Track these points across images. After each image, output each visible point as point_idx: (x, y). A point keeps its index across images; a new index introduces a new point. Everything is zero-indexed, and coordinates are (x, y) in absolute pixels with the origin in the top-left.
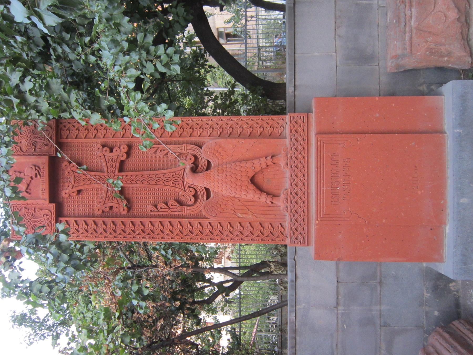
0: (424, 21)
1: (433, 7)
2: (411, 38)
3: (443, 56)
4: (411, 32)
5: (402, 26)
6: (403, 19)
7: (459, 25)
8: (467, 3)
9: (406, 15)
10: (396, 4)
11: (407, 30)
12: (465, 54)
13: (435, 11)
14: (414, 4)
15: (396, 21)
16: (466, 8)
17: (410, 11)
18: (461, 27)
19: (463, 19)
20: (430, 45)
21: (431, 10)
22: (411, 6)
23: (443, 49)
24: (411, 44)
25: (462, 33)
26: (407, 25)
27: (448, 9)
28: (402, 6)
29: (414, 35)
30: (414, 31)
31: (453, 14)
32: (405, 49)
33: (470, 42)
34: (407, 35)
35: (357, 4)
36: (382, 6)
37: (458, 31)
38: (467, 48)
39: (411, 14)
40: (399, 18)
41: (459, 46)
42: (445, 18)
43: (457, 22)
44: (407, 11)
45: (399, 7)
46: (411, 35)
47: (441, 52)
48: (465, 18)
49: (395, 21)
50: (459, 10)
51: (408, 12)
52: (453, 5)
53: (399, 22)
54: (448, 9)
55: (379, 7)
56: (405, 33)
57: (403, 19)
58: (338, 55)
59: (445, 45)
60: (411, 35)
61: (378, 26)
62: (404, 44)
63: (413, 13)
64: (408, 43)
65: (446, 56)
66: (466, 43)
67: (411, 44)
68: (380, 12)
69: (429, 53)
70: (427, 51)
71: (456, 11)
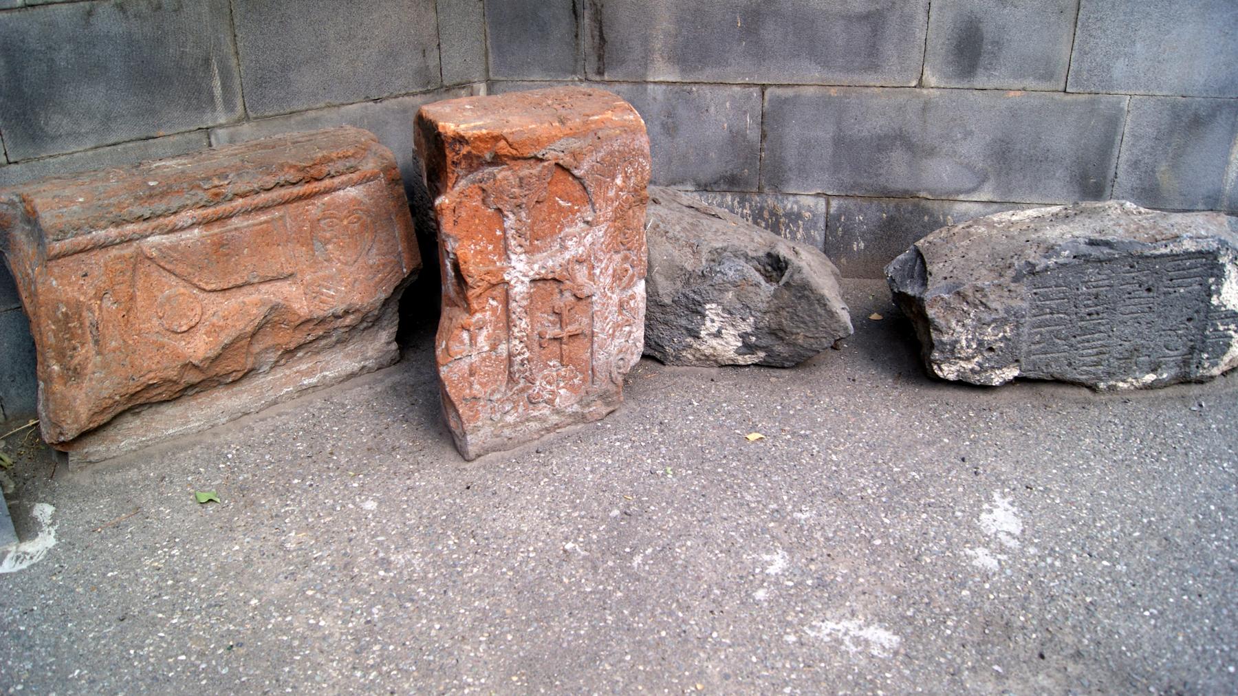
0: (164, 273)
1: (213, 286)
2: (104, 246)
3: (61, 356)
4: (122, 242)
5: (137, 210)
6: (161, 206)
7: (172, 374)
8: (240, 375)
9: (175, 213)
10: (208, 179)
11: (129, 228)
12: (84, 417)
13: (202, 295)
14: (216, 229)
15: (153, 188)
16: (228, 374)
17: (190, 222)
18: (166, 381)
19: (193, 377)
20: (90, 309)
21: (203, 285)
22: (207, 223)
23: (85, 352)
24: (81, 251)
25: (149, 387)
26: (145, 225)
27: (214, 330)
28: (203, 196)
29: (114, 252)
30: (128, 251)
31: (199, 347)
32: (62, 234)
33: (129, 417)
34: (113, 232)
35: (207, 61)
36: (213, 140)
37: (152, 375)
38: (106, 417)
39: (182, 229)
40: (163, 194)
41: (105, 394)
42: (184, 328)
43: (179, 364)
44: (190, 213)
45: (199, 187)
46: (113, 244)
47: (75, 349)
48: (198, 380)
49: (152, 184)
50: (216, 359)
51: (185, 217)
52: (225, 339)
53: (151, 196)
54: (214, 330)
55: (208, 131)
56: (117, 223)
57: (161, 206)
58: (16, 14)
59: (99, 353)
60: (113, 244)
61: (147, 138)
62: (78, 229)
63: (185, 235)
64: (83, 240)
65: (66, 368)
66: (120, 409)
67: (81, 251)
68: (193, 136)
69: (66, 315)
70: (67, 304)
71: (212, 354)
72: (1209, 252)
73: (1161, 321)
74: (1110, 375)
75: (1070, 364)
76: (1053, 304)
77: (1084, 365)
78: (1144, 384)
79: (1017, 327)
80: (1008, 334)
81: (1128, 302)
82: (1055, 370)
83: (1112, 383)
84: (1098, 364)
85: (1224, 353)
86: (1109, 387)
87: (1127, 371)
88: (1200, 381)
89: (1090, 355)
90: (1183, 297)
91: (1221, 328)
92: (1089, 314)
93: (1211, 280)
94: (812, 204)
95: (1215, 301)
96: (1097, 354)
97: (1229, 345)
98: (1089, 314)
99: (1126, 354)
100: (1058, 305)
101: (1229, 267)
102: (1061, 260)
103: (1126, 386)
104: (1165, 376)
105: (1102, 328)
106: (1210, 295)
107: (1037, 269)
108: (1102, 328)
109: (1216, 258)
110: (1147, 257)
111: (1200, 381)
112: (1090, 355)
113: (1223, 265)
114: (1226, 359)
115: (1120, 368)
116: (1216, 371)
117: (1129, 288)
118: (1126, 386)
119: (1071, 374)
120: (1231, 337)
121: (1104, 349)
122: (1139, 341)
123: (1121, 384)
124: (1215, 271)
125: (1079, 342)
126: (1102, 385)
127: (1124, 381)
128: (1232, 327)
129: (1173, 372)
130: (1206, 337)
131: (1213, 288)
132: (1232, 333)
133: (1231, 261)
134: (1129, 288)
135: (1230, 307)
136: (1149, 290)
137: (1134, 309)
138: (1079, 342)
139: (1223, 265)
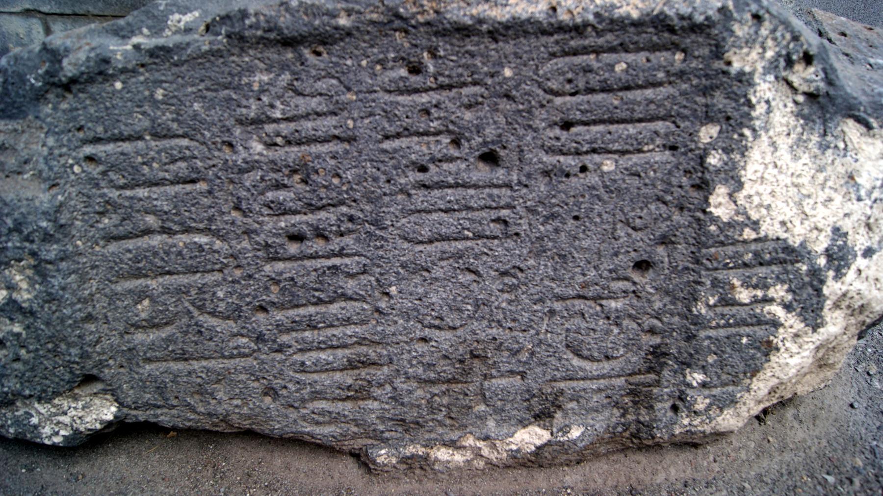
72: (695, 28)
73: (546, 267)
74: (409, 426)
75: (270, 391)
76: (161, 197)
77: (317, 395)
78: (514, 455)
79: (38, 269)
80: (24, 296)
81: (420, 198)
82: (226, 403)
83: (410, 450)
84: (359, 393)
85: (755, 372)
86: (404, 460)
87: (459, 418)
88: (690, 443)
89: (328, 368)
90: (612, 188)
91: (744, 296)
92: (297, 237)
93: (708, 133)
94: (22, 31)
95: (720, 205)
96: (352, 365)
97: (769, 348)
98: (297, 237)
99: (447, 369)
100: (176, 200)
101: (764, 89)
102: (168, 39)
103: (459, 458)
104: (575, 433)
105: (350, 286)
106: (704, 187)
107: (69, 68)
108: (350, 286)
109: (718, 52)
110: (463, 31)
111: (690, 443)
112: (328, 368)
113: (744, 79)
114: (761, 386)
115: (432, 410)
116: (728, 420)
117: (419, 149)
118: (459, 458)
119: (280, 419)
120: (776, 324)
121: (372, 353)
122: (483, 331)
123: (442, 454)
124: (719, 100)
125: (282, 329)
126: (383, 455)
127: (453, 444)
128: (779, 291)
129: (601, 422)
130: (698, 321)
131: (714, 160)
132: (779, 311)
133: (772, 67)
134: (419, 149)
135: (770, 228)
136: (490, 158)
137: (449, 223)
138: (282, 329)
139: (744, 79)
